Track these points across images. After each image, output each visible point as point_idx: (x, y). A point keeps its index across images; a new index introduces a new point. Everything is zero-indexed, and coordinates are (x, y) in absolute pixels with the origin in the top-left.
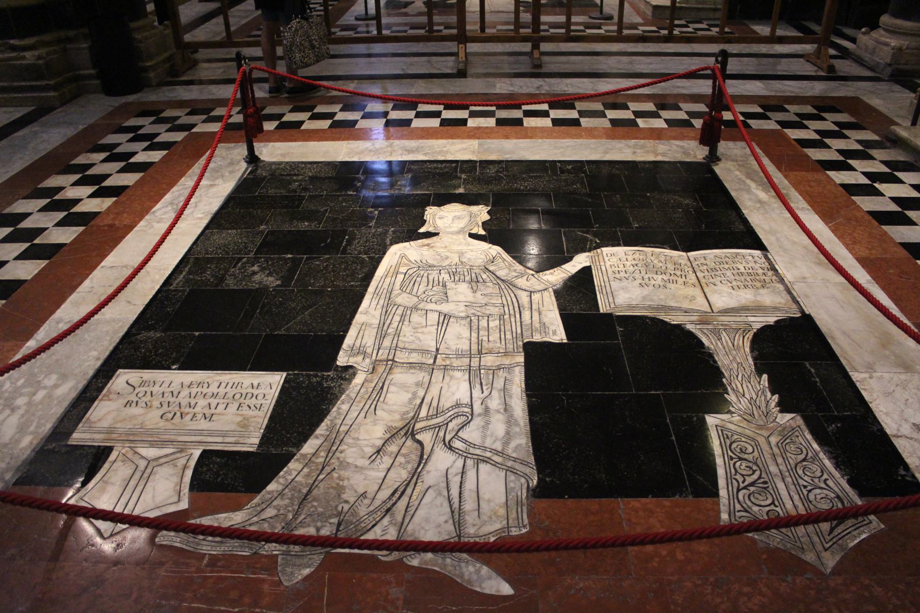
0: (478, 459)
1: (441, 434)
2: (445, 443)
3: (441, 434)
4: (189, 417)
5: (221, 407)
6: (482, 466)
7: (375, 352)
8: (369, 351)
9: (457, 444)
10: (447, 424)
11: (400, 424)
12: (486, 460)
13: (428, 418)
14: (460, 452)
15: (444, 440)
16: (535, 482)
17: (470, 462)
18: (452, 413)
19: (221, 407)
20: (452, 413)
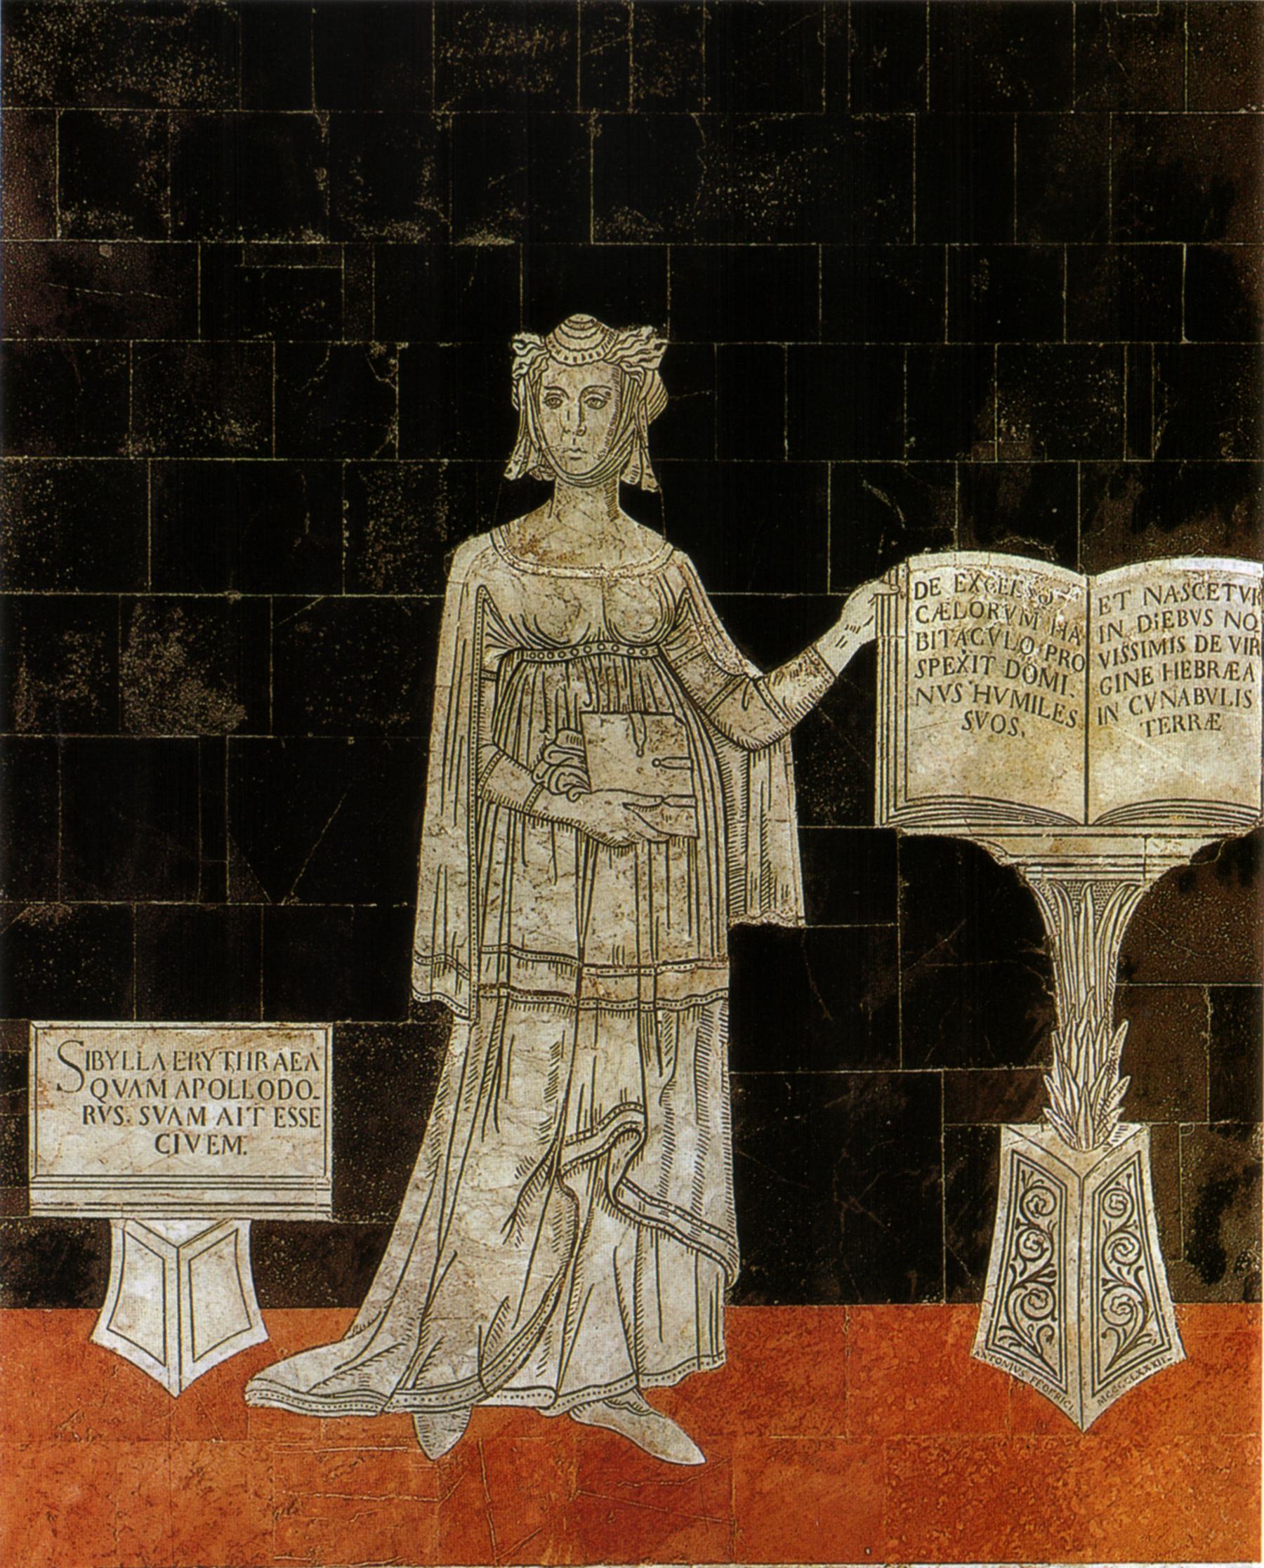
0: (658, 1228)
1: (602, 1175)
2: (608, 1196)
3: (602, 1175)
4: (203, 1144)
5: (248, 1117)
6: (664, 1242)
7: (475, 960)
8: (463, 958)
9: (628, 1198)
10: (609, 1150)
11: (538, 1153)
12: (669, 1232)
13: (581, 1137)
14: (632, 1215)
15: (606, 1189)
16: (737, 1271)
17: (645, 1234)
18: (615, 1124)
19: (248, 1117)
20: (615, 1124)
